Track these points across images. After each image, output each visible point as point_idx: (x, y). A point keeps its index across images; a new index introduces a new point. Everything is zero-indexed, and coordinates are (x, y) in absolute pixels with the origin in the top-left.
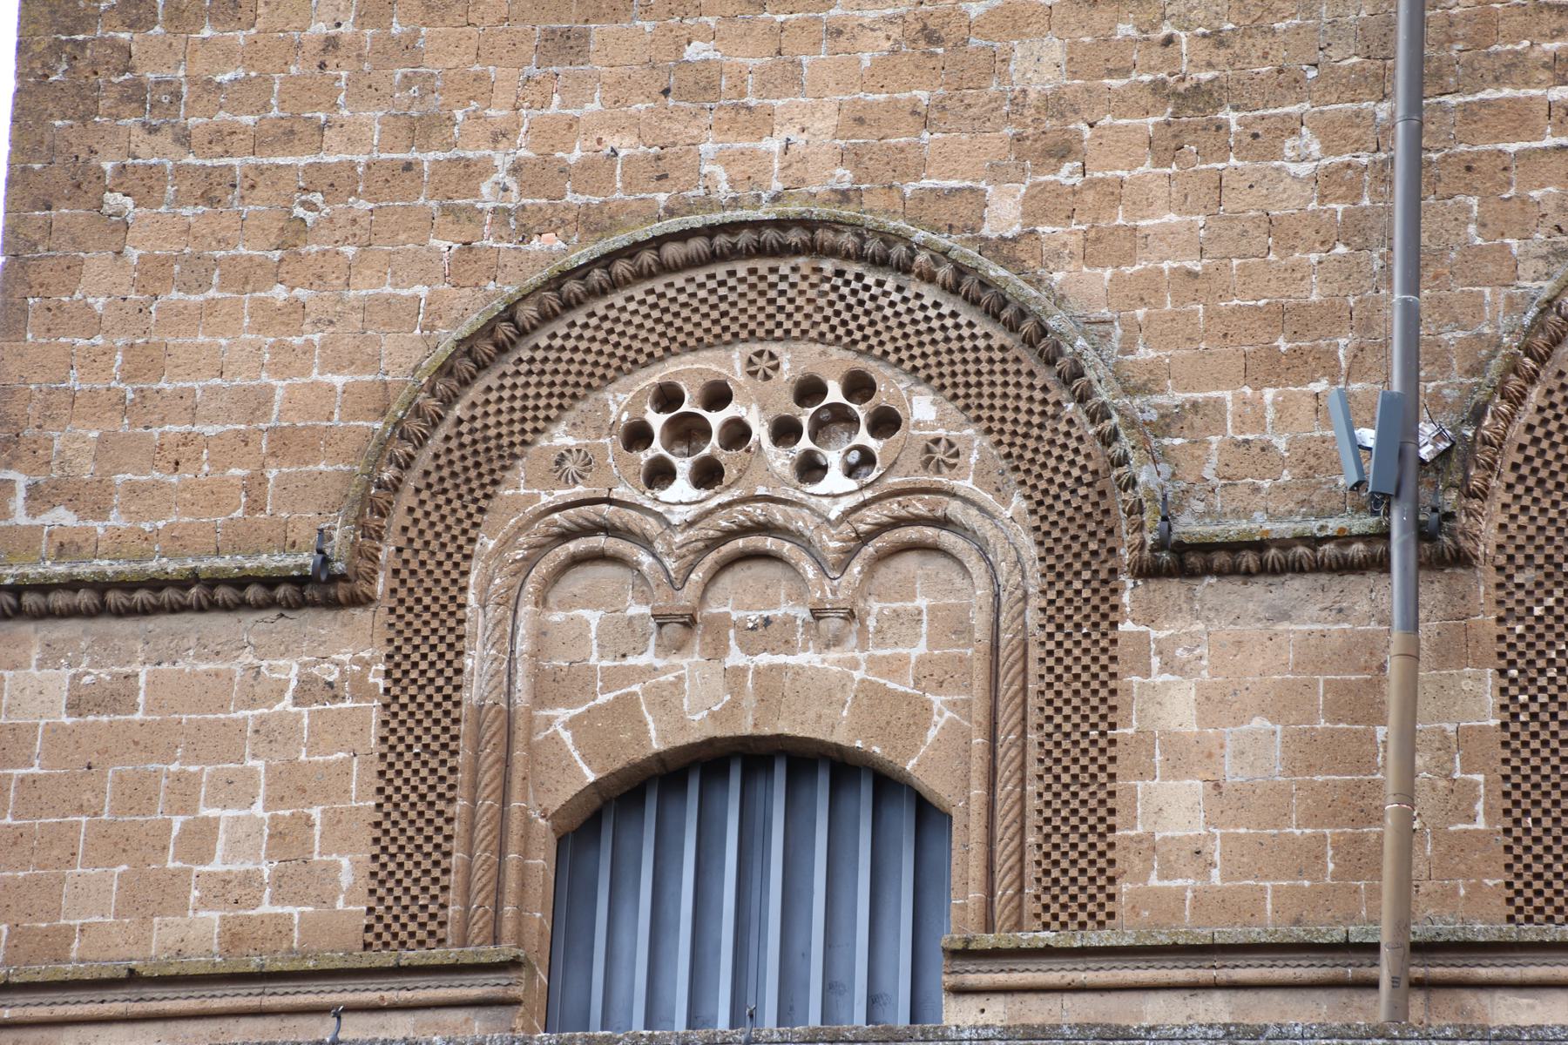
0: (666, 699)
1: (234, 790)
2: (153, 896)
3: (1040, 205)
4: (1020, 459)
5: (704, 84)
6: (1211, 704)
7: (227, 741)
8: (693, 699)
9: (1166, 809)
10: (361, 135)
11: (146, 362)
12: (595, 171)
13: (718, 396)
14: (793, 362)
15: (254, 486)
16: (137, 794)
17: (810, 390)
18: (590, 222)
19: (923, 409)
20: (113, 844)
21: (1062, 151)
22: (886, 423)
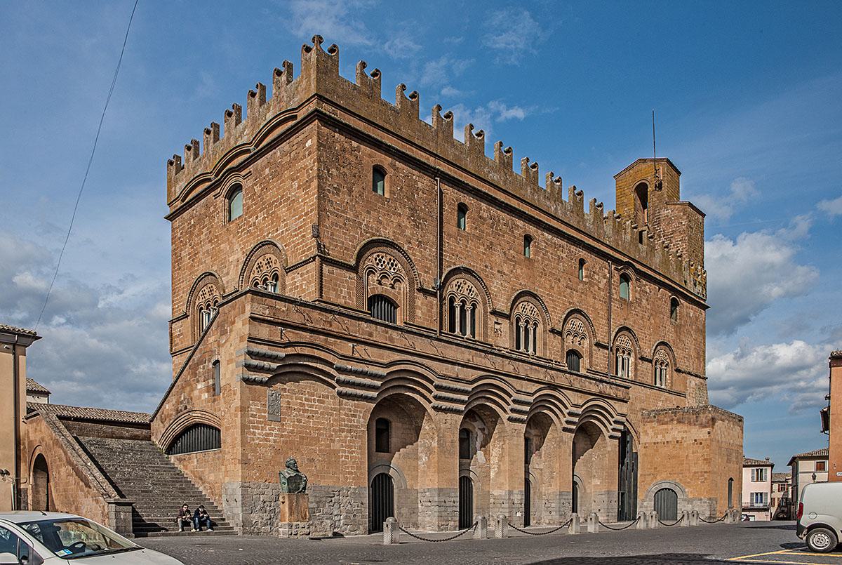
0: (377, 288)
1: (344, 287)
2: (338, 296)
3: (409, 248)
4: (407, 273)
5: (380, 222)
6: (422, 304)
7: (342, 281)
8: (379, 290)
9: (419, 313)
10: (350, 215)
11: (332, 234)
12: (372, 228)
13: (382, 257)
14: (389, 257)
15: (343, 252)
16: (335, 285)
17: (390, 260)
18: (373, 235)
19: (399, 265)
20: (334, 290)
21: (410, 243)
22: (396, 265)
